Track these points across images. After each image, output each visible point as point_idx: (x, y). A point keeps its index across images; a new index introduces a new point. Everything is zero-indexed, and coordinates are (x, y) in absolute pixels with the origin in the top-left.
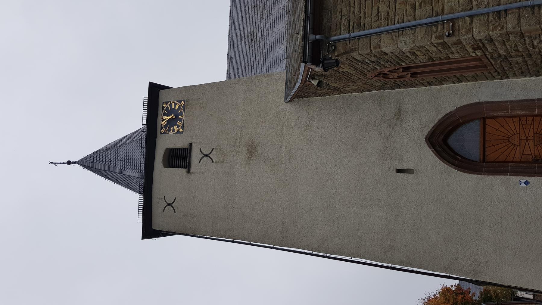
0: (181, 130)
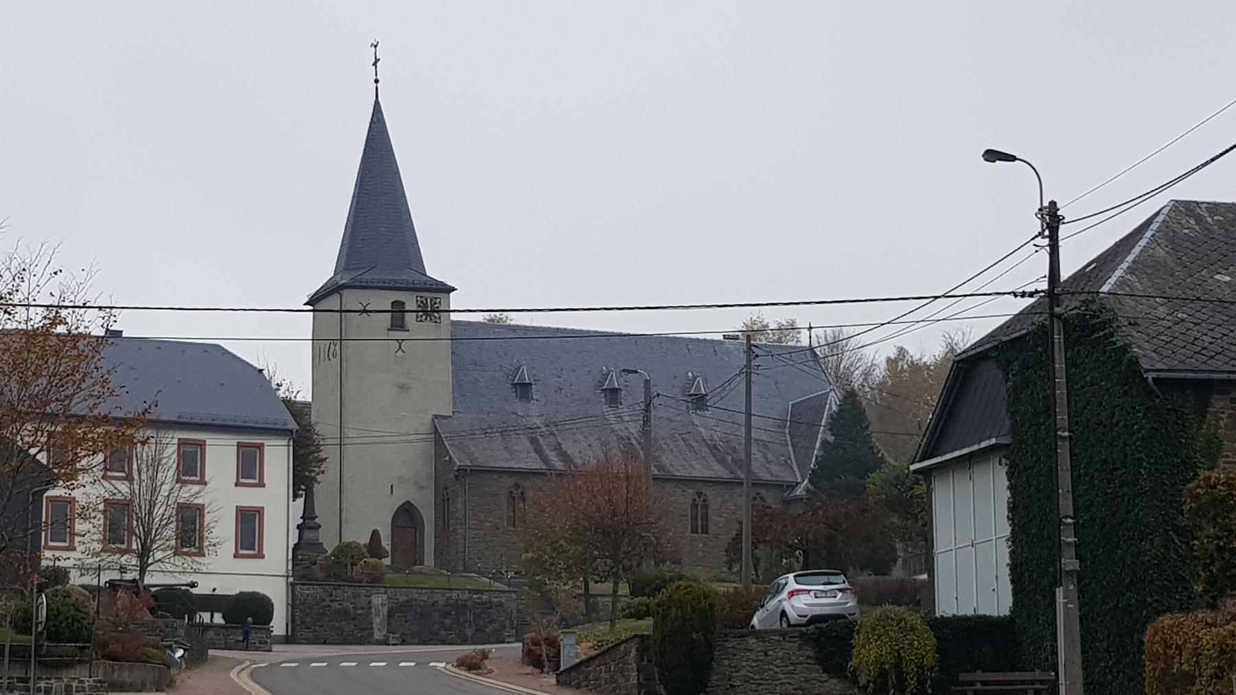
0: (419, 319)
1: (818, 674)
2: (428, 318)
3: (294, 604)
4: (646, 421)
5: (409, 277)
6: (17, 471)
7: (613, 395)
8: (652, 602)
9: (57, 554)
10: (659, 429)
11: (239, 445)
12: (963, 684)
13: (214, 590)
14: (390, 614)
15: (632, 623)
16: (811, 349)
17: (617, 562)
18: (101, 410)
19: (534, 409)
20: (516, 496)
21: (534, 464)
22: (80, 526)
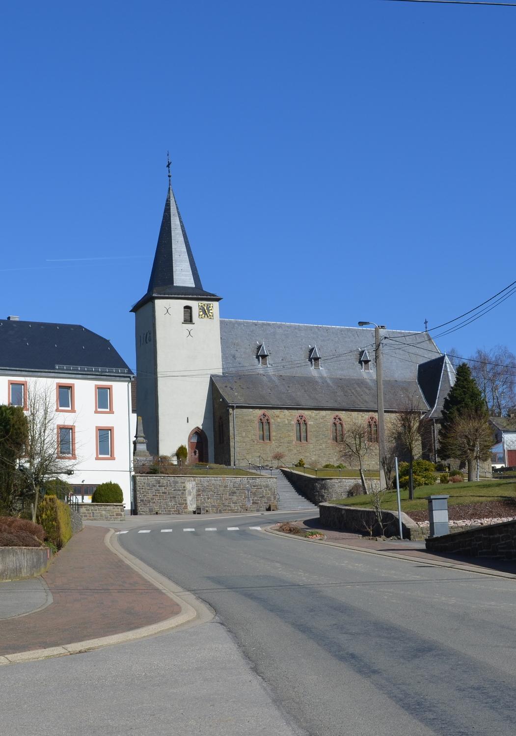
0: (200, 317)
2: (206, 316)
13: (83, 482)
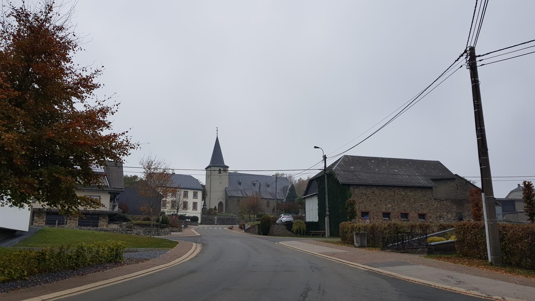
1: (287, 231)
3: (202, 218)
4: (260, 189)
5: (223, 165)
6: (157, 196)
7: (254, 184)
8: (260, 218)
9: (164, 209)
10: (262, 190)
11: (194, 192)
12: (310, 233)
14: (218, 220)
15: (257, 222)
16: (286, 178)
17: (254, 212)
18: (171, 186)
19: (241, 187)
20: (238, 201)
21: (242, 196)
22: (167, 205)
